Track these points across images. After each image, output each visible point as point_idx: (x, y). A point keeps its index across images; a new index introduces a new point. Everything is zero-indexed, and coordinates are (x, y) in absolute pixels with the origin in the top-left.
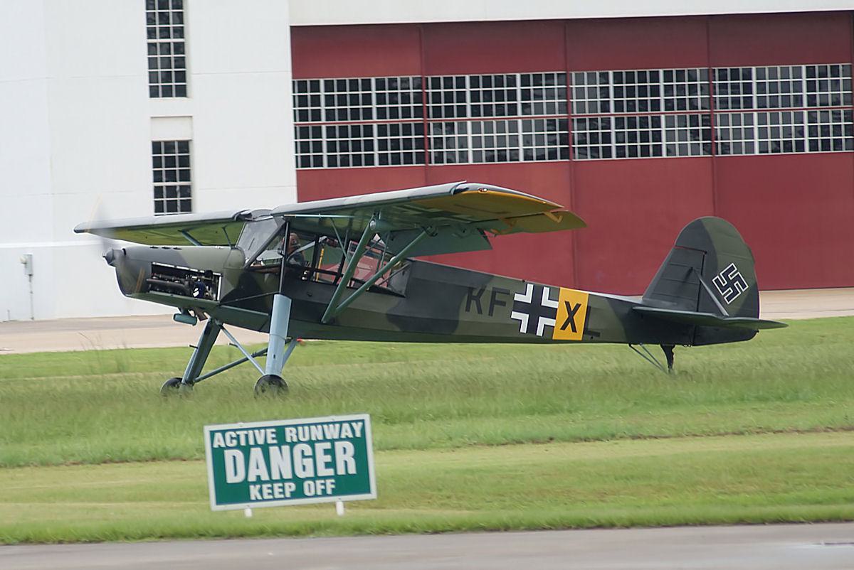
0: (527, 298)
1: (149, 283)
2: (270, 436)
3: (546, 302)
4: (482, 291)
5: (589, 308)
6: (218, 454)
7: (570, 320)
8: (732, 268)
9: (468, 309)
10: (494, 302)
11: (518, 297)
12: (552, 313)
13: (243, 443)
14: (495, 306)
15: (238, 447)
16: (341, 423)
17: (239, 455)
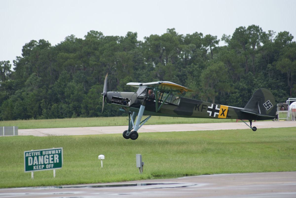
0: (212, 107)
1: (111, 101)
2: (39, 153)
3: (216, 108)
4: (200, 105)
5: (228, 111)
6: (27, 158)
7: (223, 113)
8: (269, 101)
9: (195, 110)
10: (202, 108)
11: (209, 107)
12: (218, 111)
13: (33, 155)
14: (203, 109)
15: (31, 156)
16: (56, 150)
17: (32, 158)
